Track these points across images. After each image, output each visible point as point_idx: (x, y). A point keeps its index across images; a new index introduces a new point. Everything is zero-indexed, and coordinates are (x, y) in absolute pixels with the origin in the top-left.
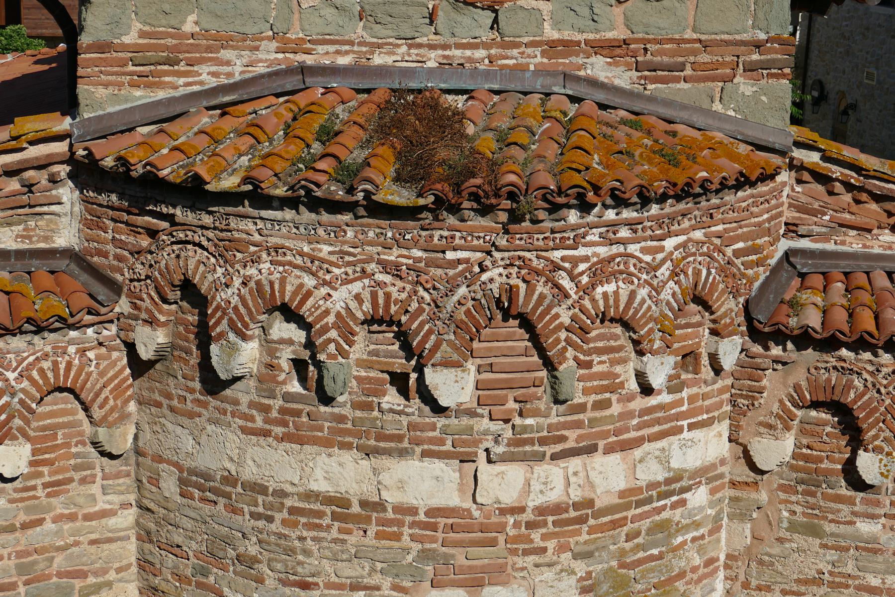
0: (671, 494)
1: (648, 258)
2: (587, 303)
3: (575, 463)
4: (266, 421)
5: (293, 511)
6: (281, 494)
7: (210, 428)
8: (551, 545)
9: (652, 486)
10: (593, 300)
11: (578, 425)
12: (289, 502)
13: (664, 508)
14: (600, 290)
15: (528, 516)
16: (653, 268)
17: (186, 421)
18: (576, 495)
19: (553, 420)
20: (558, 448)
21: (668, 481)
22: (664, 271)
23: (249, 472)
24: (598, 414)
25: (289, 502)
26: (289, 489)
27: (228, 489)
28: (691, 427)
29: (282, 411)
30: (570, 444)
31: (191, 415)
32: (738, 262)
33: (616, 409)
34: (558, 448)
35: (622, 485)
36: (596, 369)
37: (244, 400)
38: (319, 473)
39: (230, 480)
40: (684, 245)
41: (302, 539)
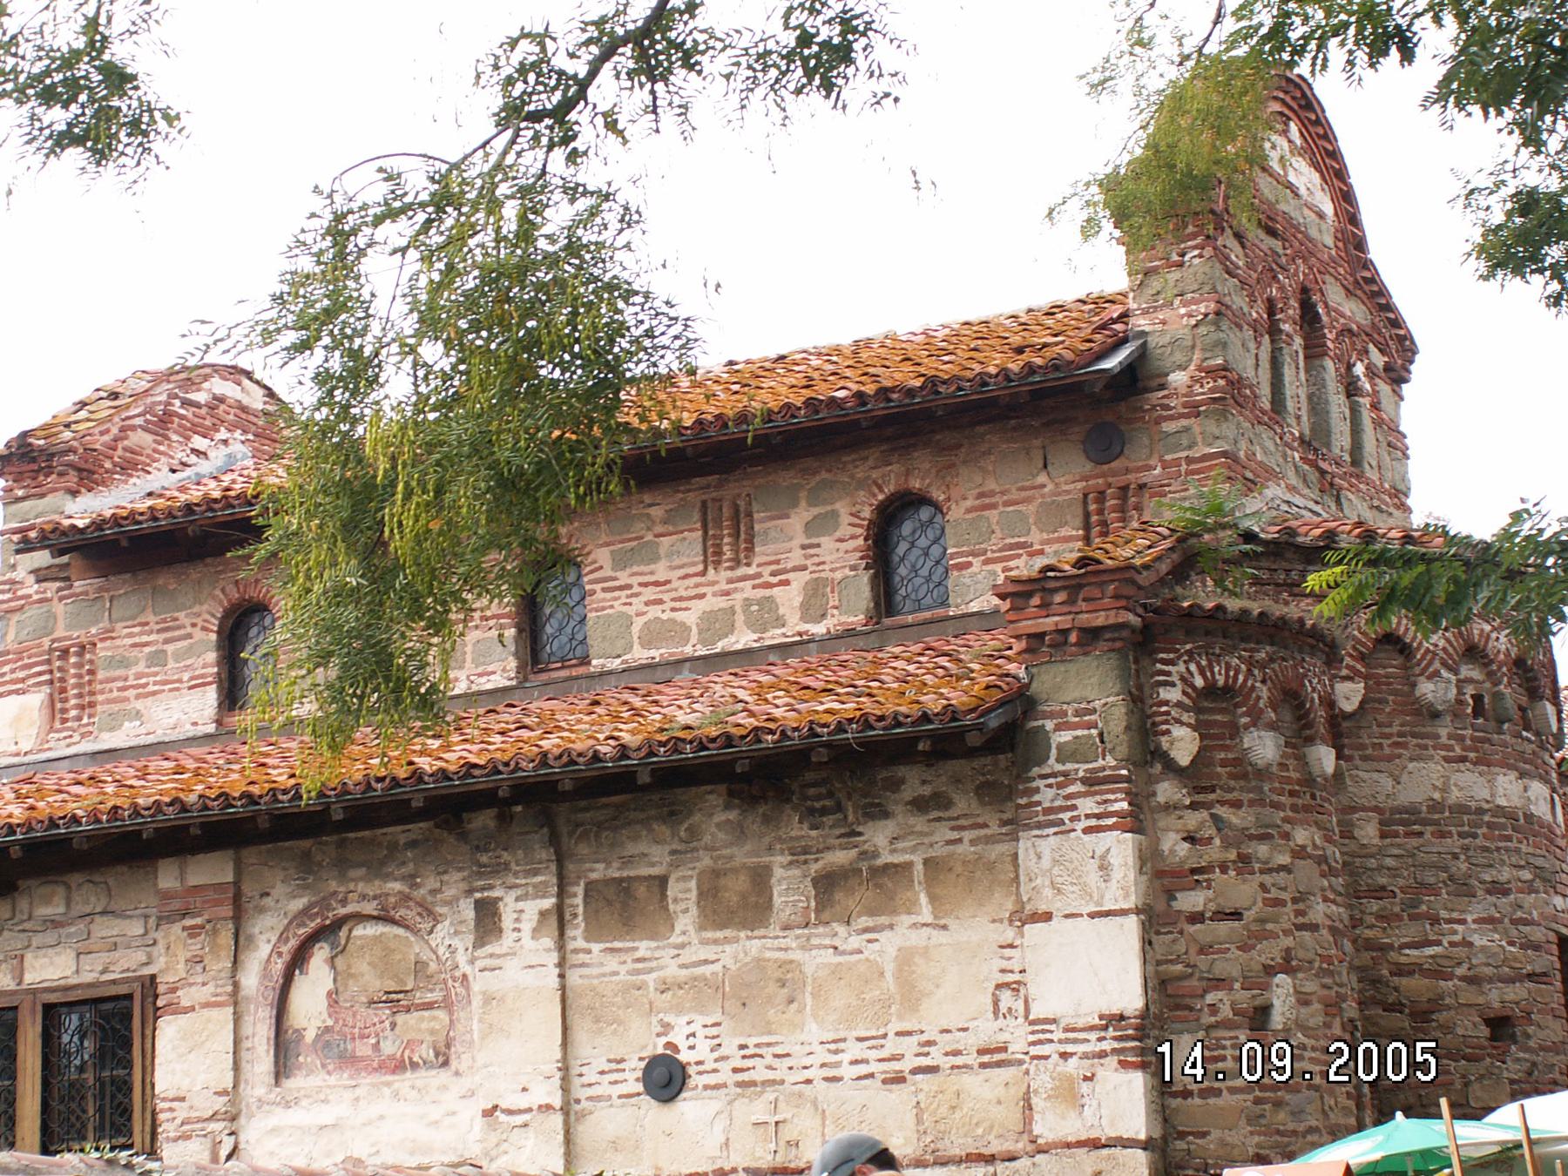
4: (1464, 749)
5: (1490, 825)
6: (1480, 811)
7: (1411, 766)
12: (1486, 818)
17: (1383, 765)
23: (1455, 795)
25: (1486, 818)
26: (1486, 806)
27: (1436, 816)
29: (1473, 739)
31: (1390, 759)
37: (1443, 732)
38: (1501, 791)
39: (1435, 806)
41: (1498, 849)
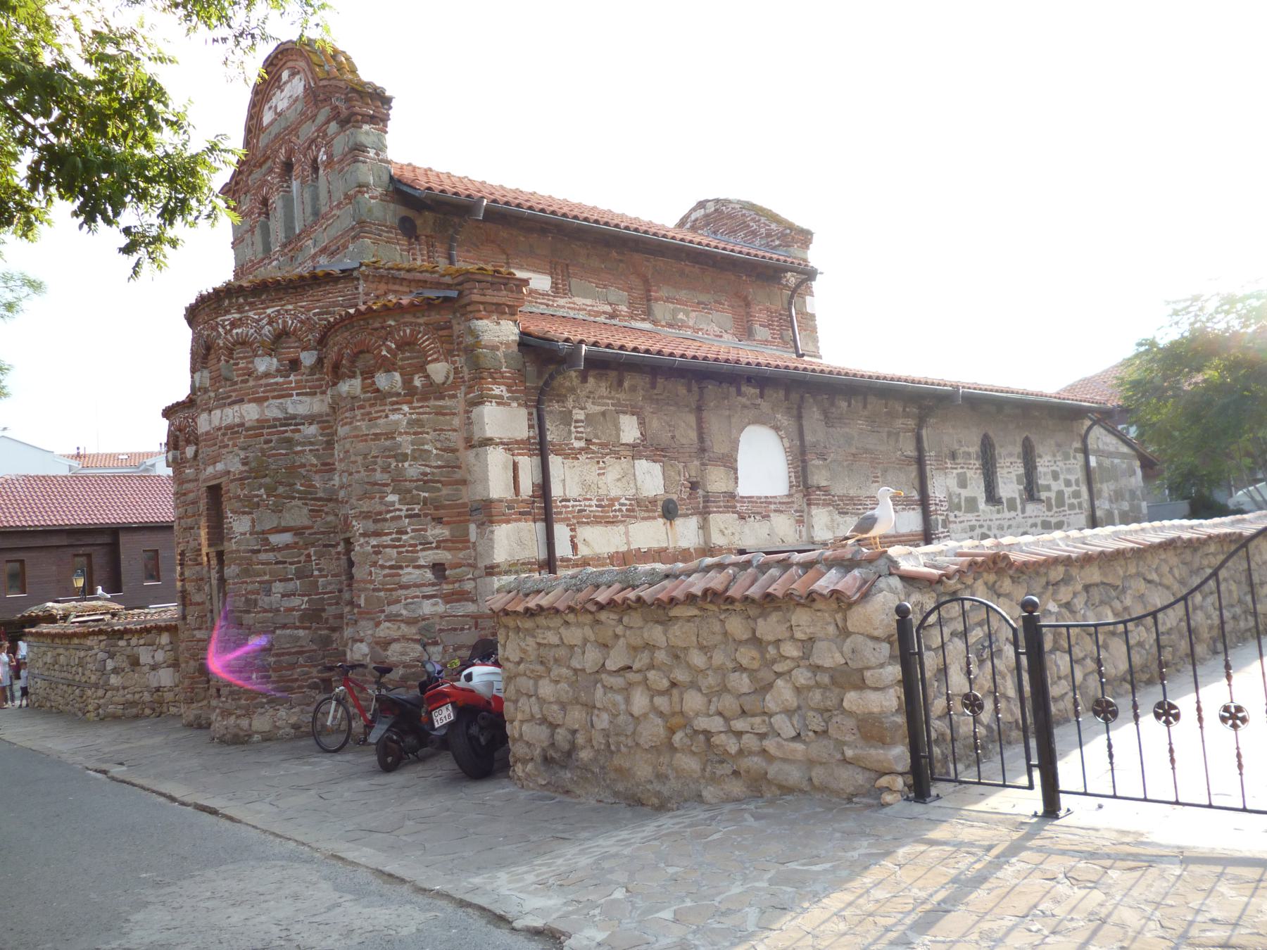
0: (290, 425)
1: (256, 317)
2: (229, 337)
3: (236, 407)
8: (230, 443)
9: (275, 419)
10: (232, 336)
11: (234, 391)
13: (286, 431)
14: (235, 331)
15: (223, 431)
16: (257, 321)
18: (237, 420)
19: (228, 389)
20: (229, 400)
21: (285, 419)
22: (265, 322)
24: (243, 385)
28: (298, 394)
30: (233, 399)
32: (316, 318)
33: (251, 383)
34: (229, 400)
35: (257, 417)
36: (240, 366)
40: (278, 311)
